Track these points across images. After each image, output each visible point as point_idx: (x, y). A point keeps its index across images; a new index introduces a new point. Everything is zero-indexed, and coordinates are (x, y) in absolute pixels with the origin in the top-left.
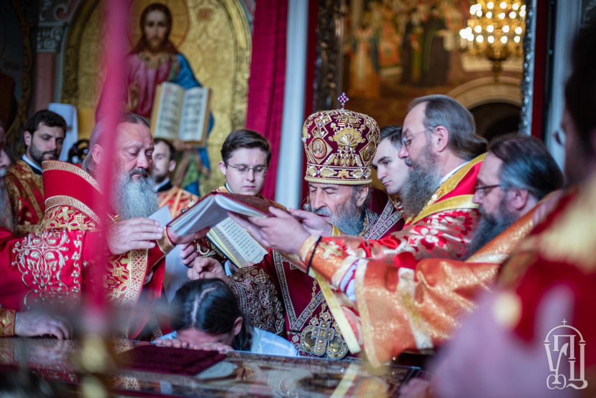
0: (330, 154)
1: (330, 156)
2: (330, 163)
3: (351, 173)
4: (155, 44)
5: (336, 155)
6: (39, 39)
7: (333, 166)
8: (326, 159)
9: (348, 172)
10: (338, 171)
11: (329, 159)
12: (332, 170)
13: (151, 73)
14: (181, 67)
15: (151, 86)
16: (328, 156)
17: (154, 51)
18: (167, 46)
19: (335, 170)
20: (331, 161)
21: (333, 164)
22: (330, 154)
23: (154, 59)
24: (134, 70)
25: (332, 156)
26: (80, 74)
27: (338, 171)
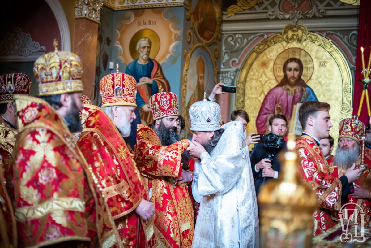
4: (292, 81)
6: (221, 78)
13: (290, 98)
14: (308, 94)
15: (290, 105)
17: (292, 85)
18: (300, 82)
23: (292, 90)
24: (279, 96)
26: (246, 98)
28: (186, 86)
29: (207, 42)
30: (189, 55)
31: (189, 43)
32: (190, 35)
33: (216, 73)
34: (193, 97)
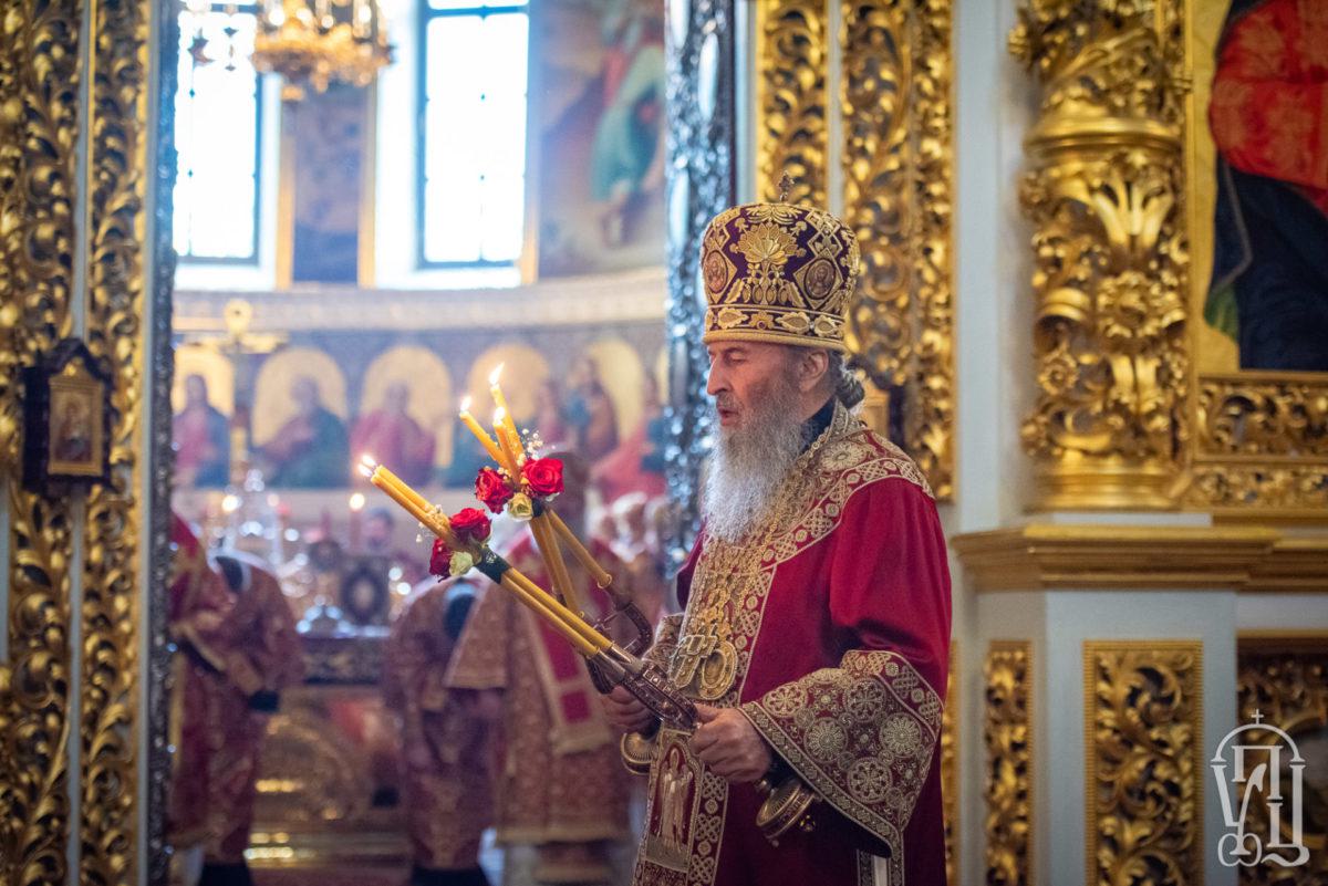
0: (734, 281)
1: (735, 284)
2: (735, 300)
3: (778, 320)
5: (745, 281)
7: (737, 305)
8: (728, 291)
9: (771, 317)
10: (749, 314)
11: (732, 290)
12: (738, 312)
16: (731, 286)
19: (743, 313)
20: (738, 295)
21: (740, 300)
22: (734, 281)
25: (740, 284)
27: (749, 314)
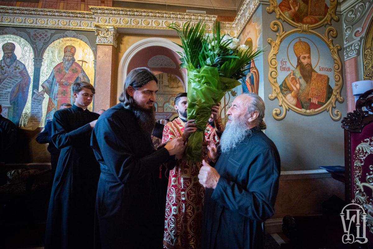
28: (276, 68)
29: (310, 26)
30: (277, 41)
31: (277, 31)
32: (275, 24)
33: (336, 50)
34: (292, 76)
